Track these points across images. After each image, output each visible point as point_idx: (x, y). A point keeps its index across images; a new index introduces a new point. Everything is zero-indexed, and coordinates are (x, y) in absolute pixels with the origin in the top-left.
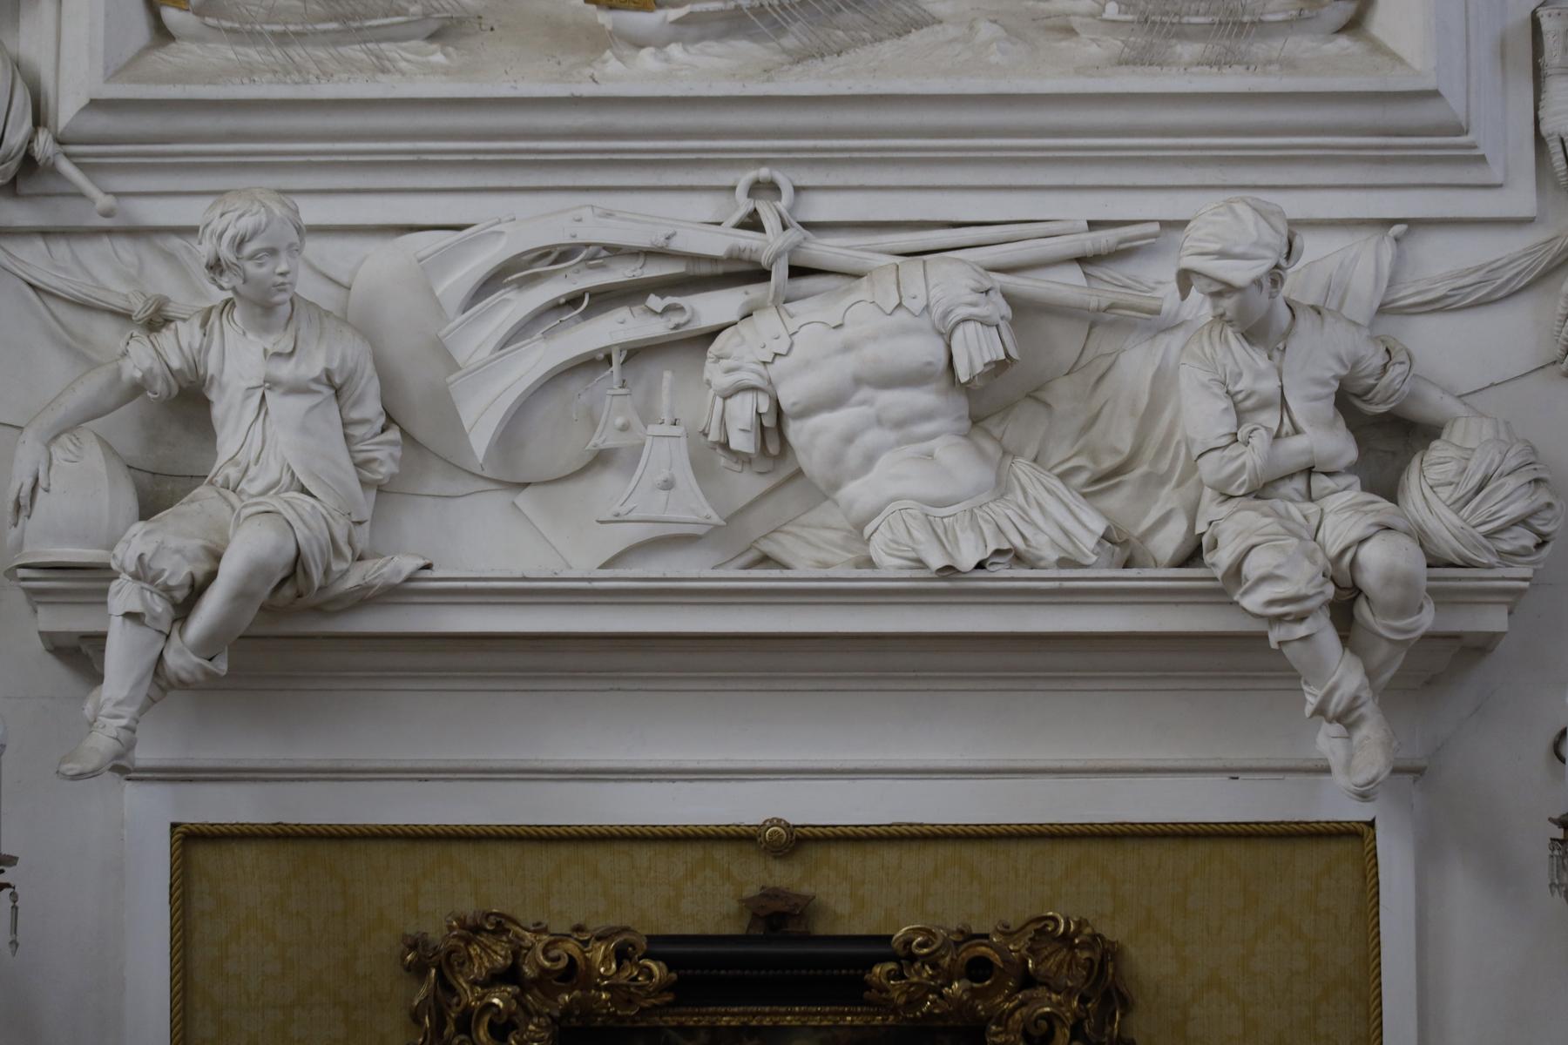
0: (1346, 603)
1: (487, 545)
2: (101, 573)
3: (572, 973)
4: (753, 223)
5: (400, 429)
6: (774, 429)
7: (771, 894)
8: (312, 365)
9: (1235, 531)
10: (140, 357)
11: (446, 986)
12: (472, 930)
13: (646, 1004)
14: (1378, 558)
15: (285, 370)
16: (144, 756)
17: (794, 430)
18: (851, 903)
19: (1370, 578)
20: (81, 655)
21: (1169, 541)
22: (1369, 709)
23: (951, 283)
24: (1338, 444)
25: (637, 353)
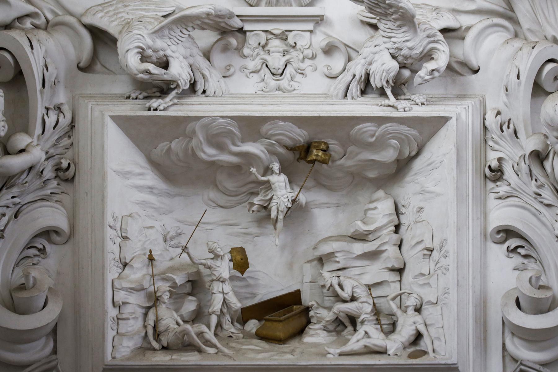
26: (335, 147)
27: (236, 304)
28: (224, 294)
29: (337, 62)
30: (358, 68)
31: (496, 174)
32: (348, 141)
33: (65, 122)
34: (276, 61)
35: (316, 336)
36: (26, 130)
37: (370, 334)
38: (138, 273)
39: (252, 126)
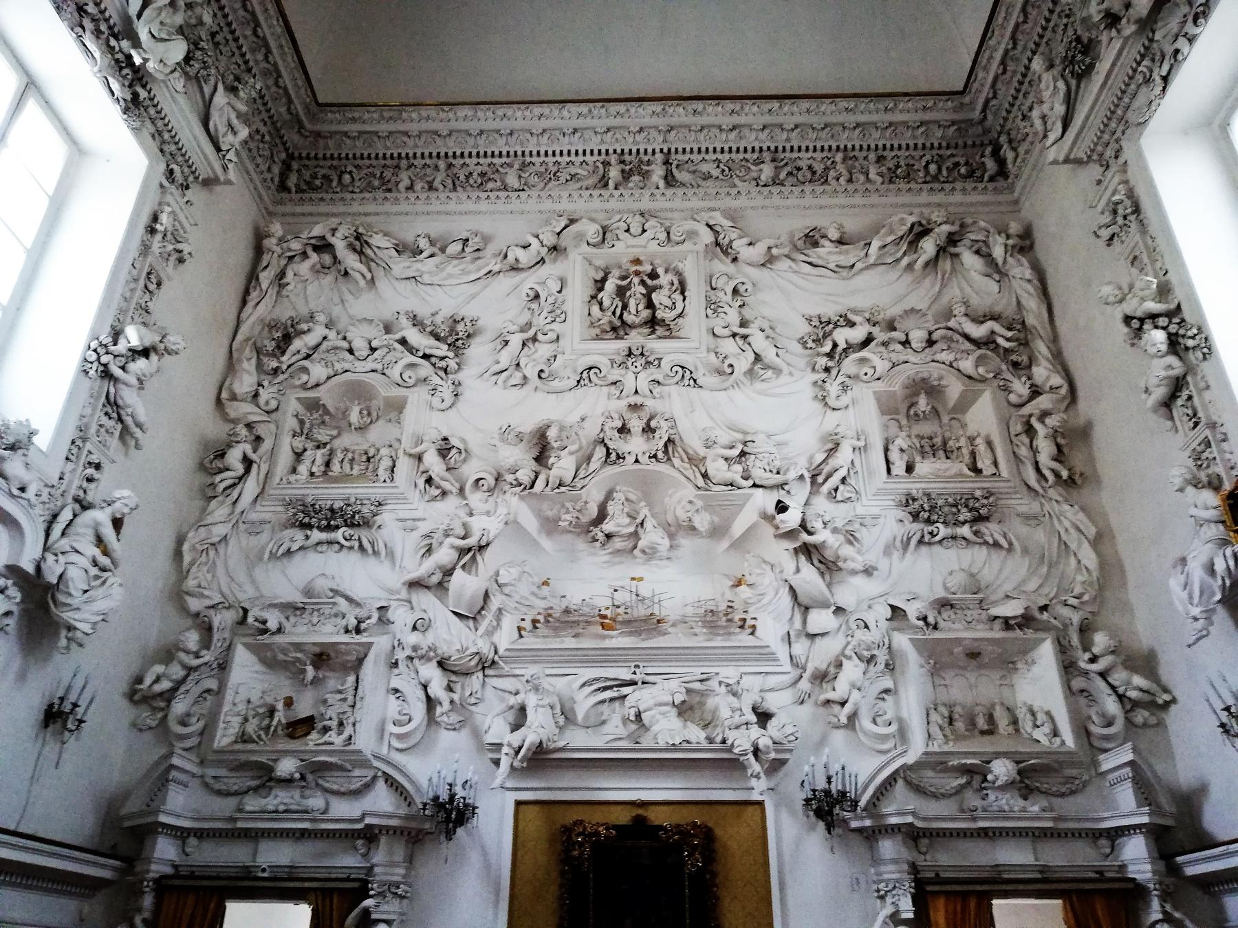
0: (756, 751)
1: (579, 740)
2: (501, 745)
3: (597, 833)
4: (634, 673)
5: (567, 716)
6: (638, 715)
7: (638, 816)
8: (546, 701)
9: (731, 736)
10: (512, 700)
11: (570, 837)
12: (576, 823)
14: (764, 742)
15: (541, 703)
16: (508, 785)
17: (643, 715)
18: (657, 817)
19: (761, 746)
20: (497, 763)
21: (719, 739)
22: (762, 775)
23: (674, 684)
24: (754, 718)
25: (612, 700)
26: (332, 654)
27: (284, 721)
28: (280, 716)
29: (339, 620)
30: (344, 622)
31: (396, 665)
32: (338, 652)
33: (226, 644)
34: (315, 620)
35: (314, 735)
36: (208, 648)
37: (332, 736)
38: (241, 707)
39: (298, 646)
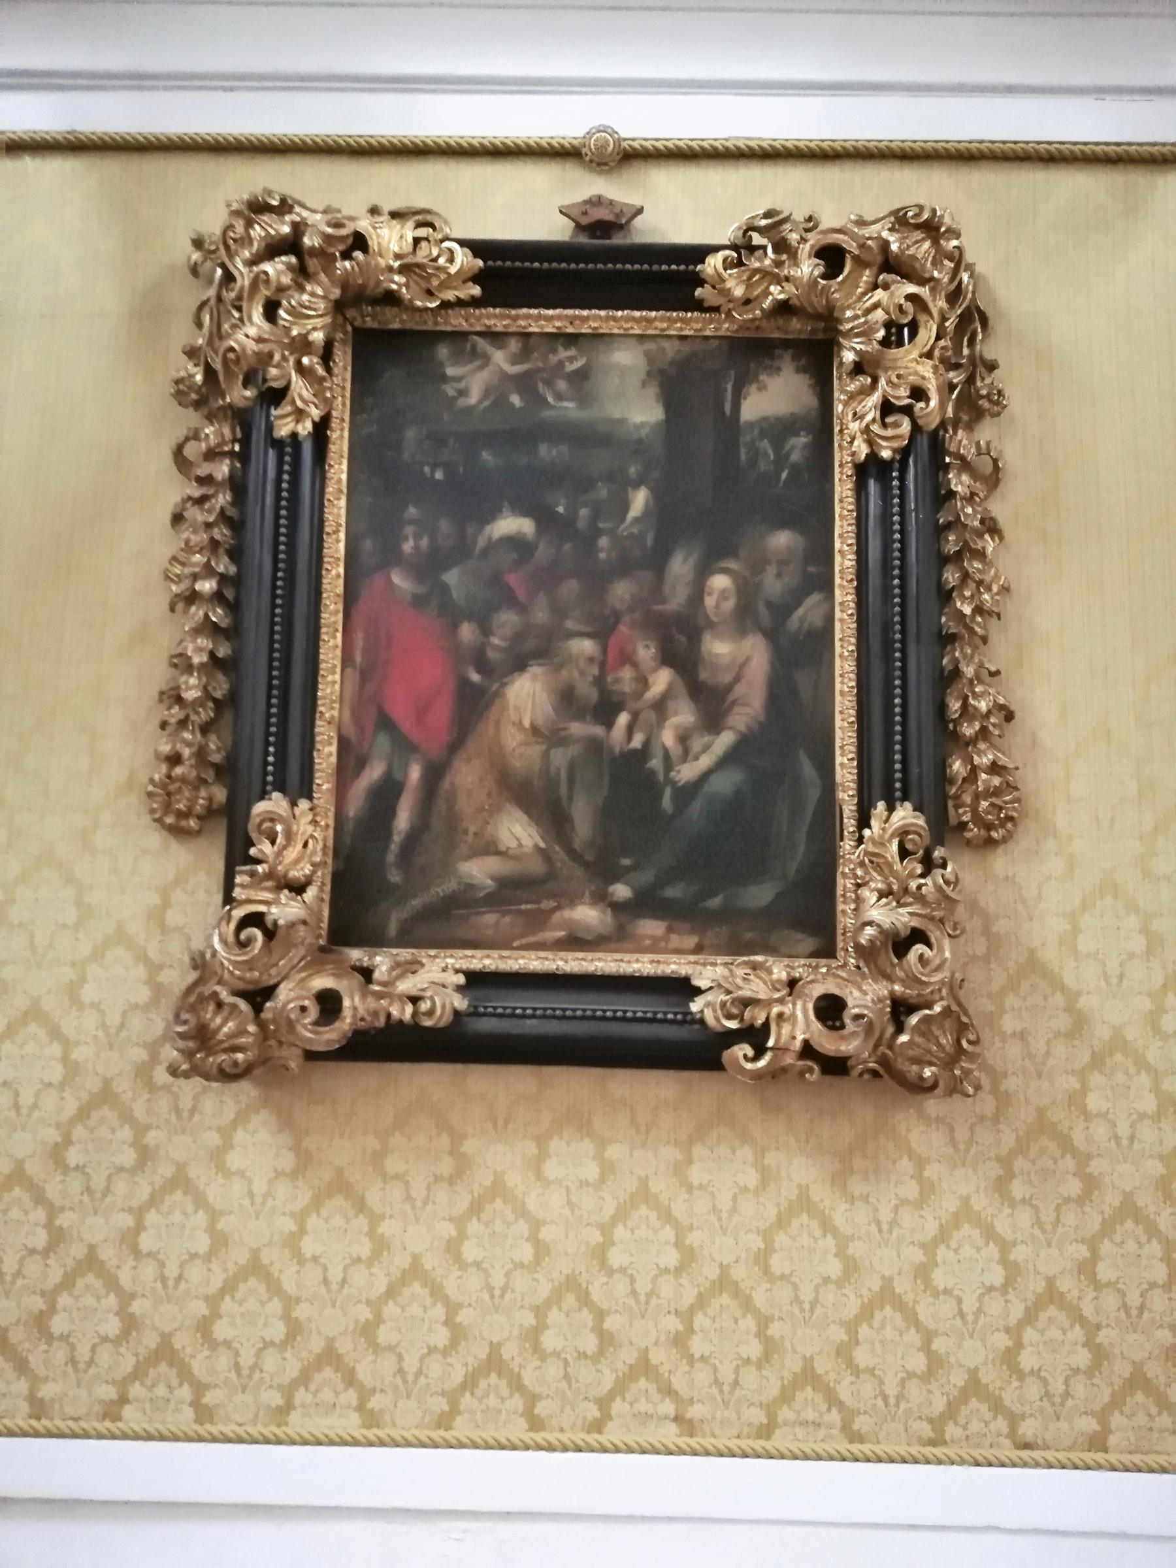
7: (597, 202)
13: (450, 295)
